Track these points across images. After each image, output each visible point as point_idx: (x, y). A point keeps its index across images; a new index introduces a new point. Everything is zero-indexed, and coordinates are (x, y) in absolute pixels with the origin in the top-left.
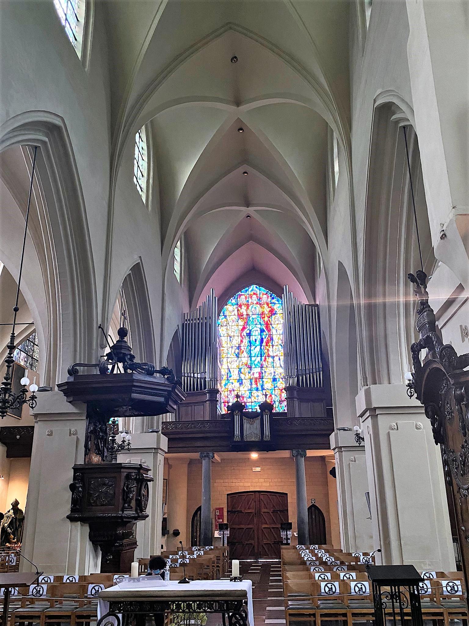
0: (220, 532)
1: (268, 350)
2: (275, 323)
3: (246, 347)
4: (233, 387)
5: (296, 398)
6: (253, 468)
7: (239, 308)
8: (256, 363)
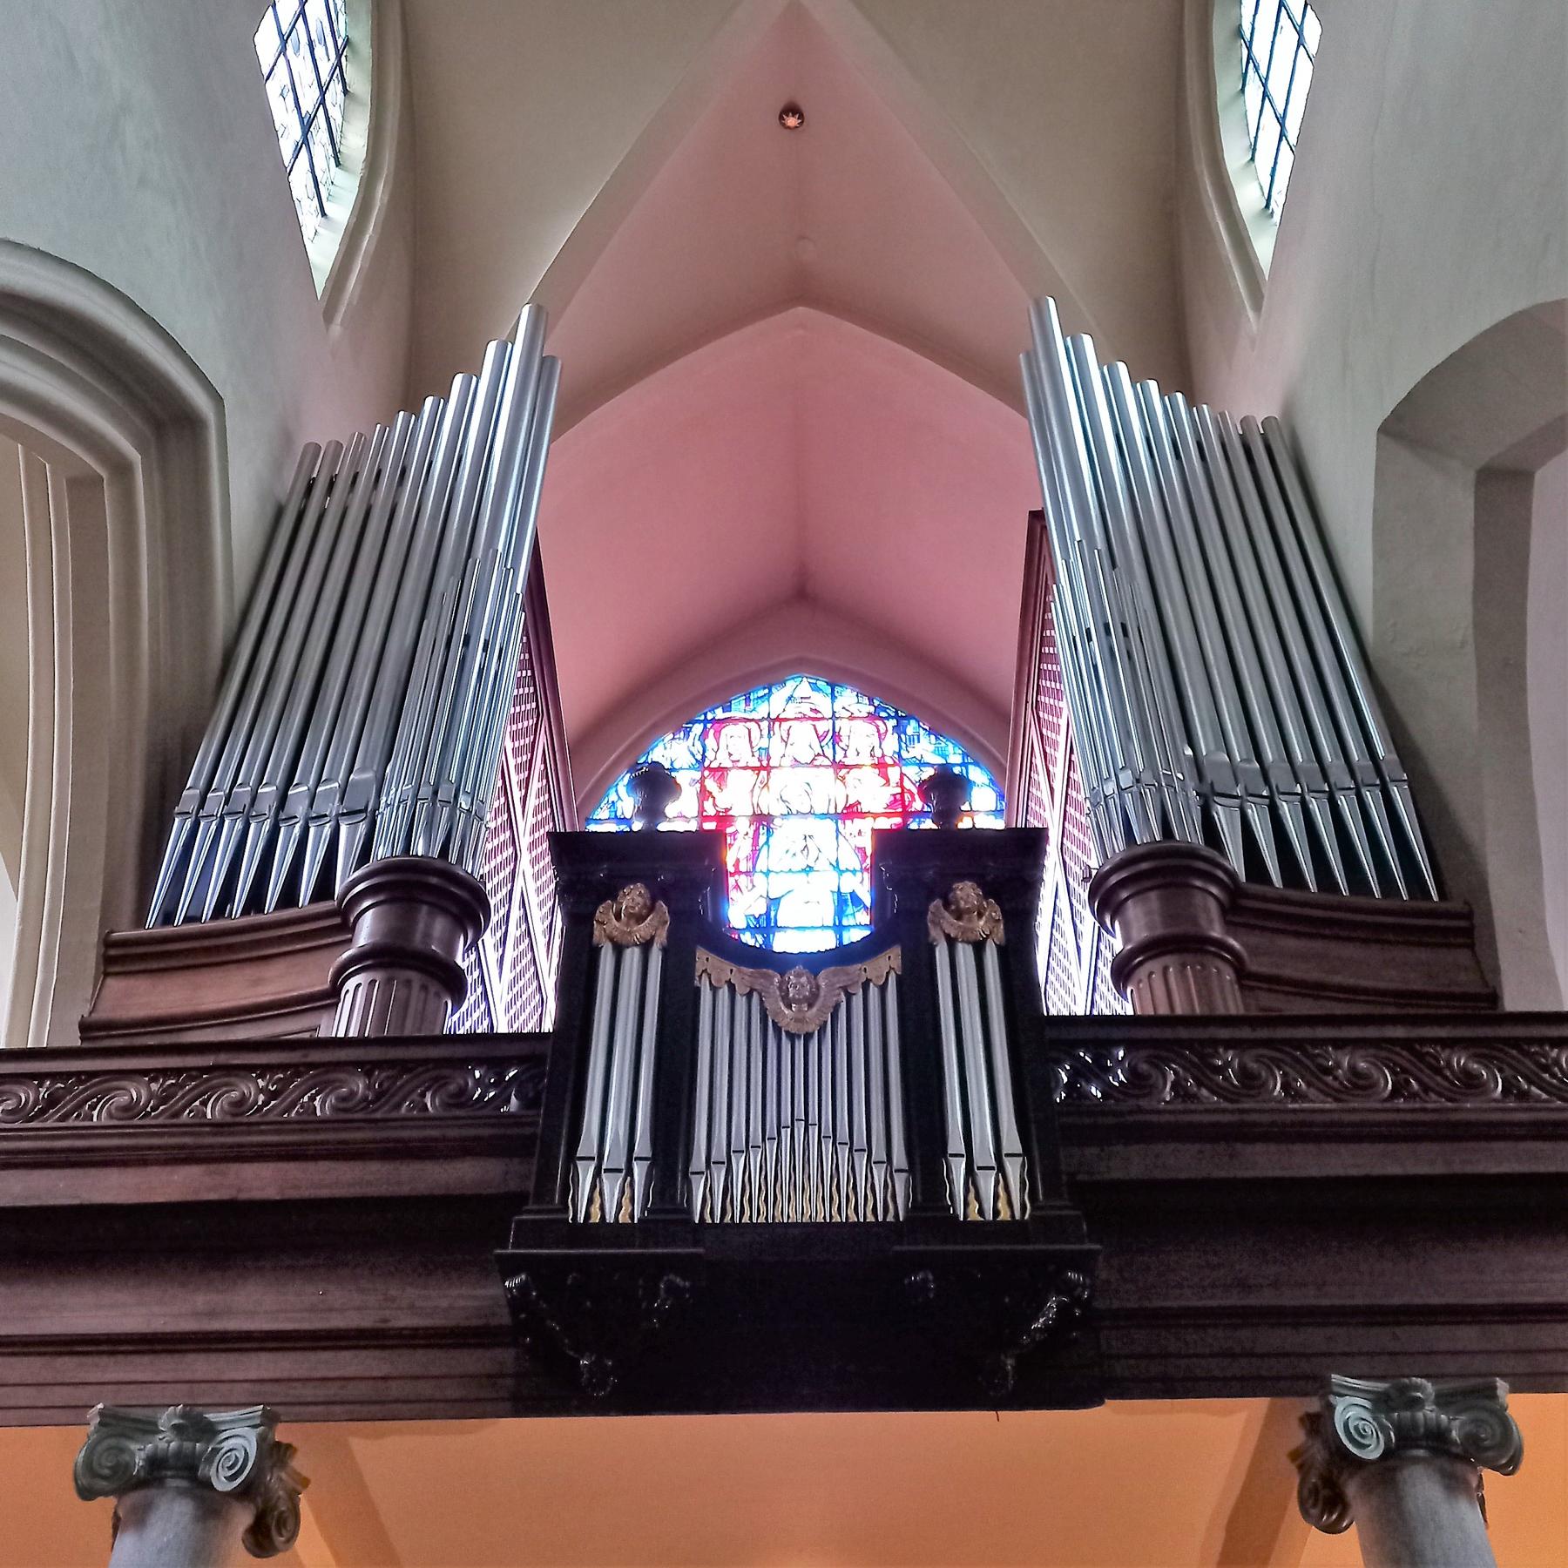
7: (711, 785)
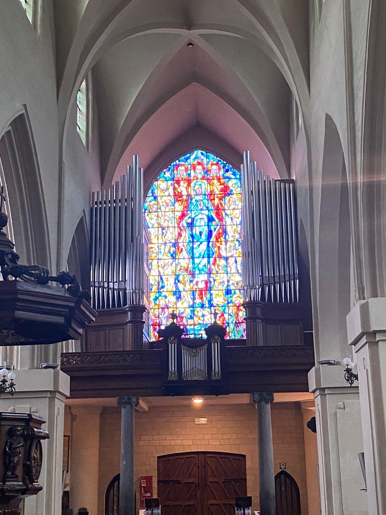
0: (147, 512)
1: (219, 248)
2: (230, 208)
3: (187, 243)
4: (167, 302)
5: (259, 318)
6: (196, 420)
8: (201, 266)
